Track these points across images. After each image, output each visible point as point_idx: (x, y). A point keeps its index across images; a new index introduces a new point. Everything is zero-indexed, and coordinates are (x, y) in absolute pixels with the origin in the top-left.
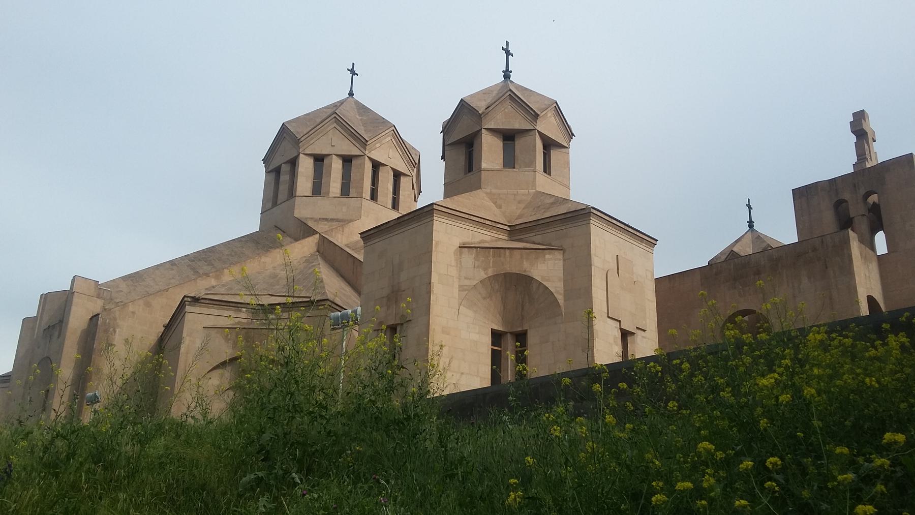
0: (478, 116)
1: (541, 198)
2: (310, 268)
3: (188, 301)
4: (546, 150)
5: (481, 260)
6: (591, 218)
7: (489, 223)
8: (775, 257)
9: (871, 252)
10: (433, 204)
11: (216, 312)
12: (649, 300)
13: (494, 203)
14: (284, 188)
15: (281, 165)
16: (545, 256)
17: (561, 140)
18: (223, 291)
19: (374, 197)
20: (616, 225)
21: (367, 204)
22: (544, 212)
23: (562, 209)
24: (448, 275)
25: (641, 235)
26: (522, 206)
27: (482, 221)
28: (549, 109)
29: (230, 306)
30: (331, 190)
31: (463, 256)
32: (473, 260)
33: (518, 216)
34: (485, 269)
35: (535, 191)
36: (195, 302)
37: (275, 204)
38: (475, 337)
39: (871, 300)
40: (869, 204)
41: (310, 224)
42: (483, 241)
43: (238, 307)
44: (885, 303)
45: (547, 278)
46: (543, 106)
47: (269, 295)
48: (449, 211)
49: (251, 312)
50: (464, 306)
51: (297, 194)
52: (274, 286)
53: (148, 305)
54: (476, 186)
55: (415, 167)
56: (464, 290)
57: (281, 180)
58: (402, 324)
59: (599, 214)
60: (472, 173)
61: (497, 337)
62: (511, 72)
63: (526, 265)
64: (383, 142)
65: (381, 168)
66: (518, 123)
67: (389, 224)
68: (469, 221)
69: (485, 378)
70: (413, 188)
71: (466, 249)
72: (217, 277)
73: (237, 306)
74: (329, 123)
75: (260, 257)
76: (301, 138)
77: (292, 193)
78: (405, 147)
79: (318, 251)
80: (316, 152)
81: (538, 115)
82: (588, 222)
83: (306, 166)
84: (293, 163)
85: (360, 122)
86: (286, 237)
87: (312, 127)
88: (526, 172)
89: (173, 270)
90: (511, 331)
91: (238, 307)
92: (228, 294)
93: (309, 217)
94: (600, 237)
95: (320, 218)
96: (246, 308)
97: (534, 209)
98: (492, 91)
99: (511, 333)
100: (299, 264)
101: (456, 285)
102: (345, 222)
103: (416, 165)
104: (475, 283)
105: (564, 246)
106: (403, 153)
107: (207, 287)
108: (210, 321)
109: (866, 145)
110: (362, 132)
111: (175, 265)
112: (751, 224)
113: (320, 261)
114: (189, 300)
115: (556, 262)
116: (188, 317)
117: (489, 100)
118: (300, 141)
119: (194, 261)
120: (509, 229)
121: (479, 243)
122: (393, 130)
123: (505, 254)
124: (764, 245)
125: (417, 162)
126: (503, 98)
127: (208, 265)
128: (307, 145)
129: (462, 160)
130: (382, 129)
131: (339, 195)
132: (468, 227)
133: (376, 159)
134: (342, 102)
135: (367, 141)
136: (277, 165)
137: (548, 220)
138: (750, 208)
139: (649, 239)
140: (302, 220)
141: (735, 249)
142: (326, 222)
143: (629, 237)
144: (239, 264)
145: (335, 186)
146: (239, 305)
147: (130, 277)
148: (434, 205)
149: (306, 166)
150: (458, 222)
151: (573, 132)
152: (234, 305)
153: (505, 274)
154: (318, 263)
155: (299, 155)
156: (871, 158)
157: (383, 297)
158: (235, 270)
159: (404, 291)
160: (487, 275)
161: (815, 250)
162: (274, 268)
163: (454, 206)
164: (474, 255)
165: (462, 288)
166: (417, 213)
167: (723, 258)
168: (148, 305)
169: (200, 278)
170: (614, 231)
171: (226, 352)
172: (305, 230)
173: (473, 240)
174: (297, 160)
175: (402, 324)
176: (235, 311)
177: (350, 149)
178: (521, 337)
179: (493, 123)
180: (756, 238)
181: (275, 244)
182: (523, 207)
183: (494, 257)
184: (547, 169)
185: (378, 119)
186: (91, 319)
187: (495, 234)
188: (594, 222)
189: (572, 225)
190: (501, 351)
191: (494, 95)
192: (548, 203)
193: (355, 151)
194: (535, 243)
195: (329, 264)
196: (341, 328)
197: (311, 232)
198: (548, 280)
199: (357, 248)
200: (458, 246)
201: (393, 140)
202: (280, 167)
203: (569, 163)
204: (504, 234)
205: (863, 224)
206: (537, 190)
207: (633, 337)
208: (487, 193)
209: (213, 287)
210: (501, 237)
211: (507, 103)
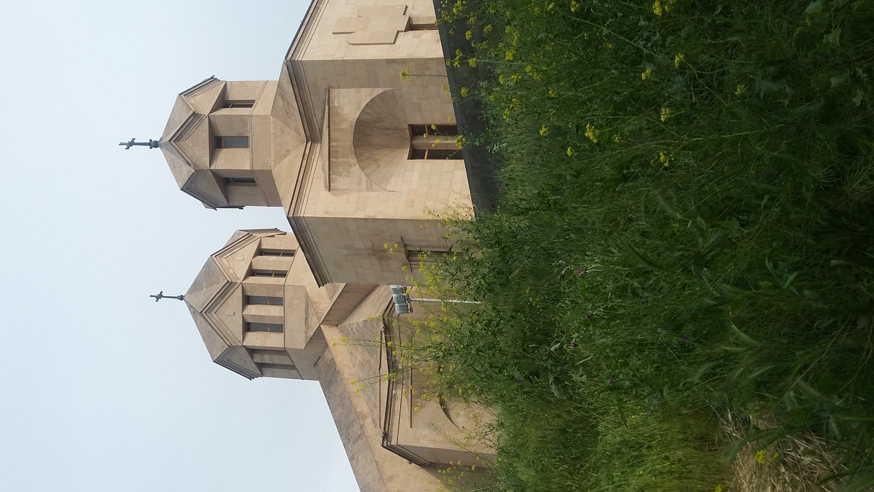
1: (277, 109)
2: (354, 333)
3: (387, 443)
5: (342, 170)
6: (296, 59)
7: (305, 162)
10: (288, 218)
11: (396, 417)
13: (285, 158)
14: (277, 360)
15: (255, 362)
16: (336, 107)
17: (217, 91)
19: (283, 274)
20: (302, 35)
21: (290, 280)
22: (292, 107)
23: (289, 89)
25: (312, 9)
26: (286, 128)
27: (303, 169)
28: (187, 101)
31: (338, 188)
32: (342, 177)
33: (296, 133)
34: (351, 166)
35: (271, 117)
36: (388, 436)
37: (293, 367)
42: (323, 169)
43: (392, 397)
47: (380, 369)
48: (294, 201)
51: (283, 346)
52: (371, 365)
53: (391, 479)
54: (268, 175)
55: (252, 235)
56: (371, 185)
57: (269, 362)
58: (405, 245)
59: (292, 52)
60: (256, 181)
61: (416, 154)
62: (151, 140)
63: (345, 126)
64: (227, 265)
65: (254, 268)
66: (203, 133)
67: (309, 259)
68: (303, 182)
69: (455, 166)
70: (273, 236)
71: (331, 184)
72: (364, 417)
73: (390, 398)
74: (211, 319)
75: (344, 379)
77: (282, 352)
80: (241, 330)
81: (194, 113)
82: (300, 63)
83: (255, 339)
84: (252, 351)
85: (208, 289)
86: (324, 356)
87: (216, 334)
89: (358, 457)
90: (410, 141)
91: (392, 397)
92: (380, 407)
93: (304, 335)
95: (306, 324)
96: (392, 390)
97: (289, 117)
98: (171, 160)
99: (412, 140)
101: (366, 194)
102: (308, 301)
103: (250, 234)
104: (364, 177)
105: (326, 88)
106: (238, 247)
107: (374, 426)
108: (406, 422)
113: (347, 323)
114: (385, 442)
115: (341, 95)
116: (402, 442)
117: (181, 162)
120: (310, 142)
121: (325, 171)
126: (177, 148)
127: (352, 426)
128: (234, 338)
129: (244, 189)
131: (282, 307)
132: (310, 183)
134: (190, 307)
135: (228, 281)
142: (309, 319)
143: (314, 21)
144: (351, 398)
145: (272, 312)
146: (390, 396)
148: (289, 216)
149: (255, 339)
150: (304, 192)
151: (210, 77)
152: (390, 402)
154: (349, 326)
155: (245, 347)
157: (380, 263)
158: (356, 401)
159: (373, 244)
160: (356, 164)
163: (289, 196)
164: (337, 177)
165: (369, 188)
166: (297, 233)
168: (391, 479)
169: (366, 433)
171: (434, 406)
174: (249, 348)
175: (405, 245)
176: (395, 400)
177: (237, 296)
178: (416, 131)
179: (204, 159)
181: (332, 366)
182: (287, 128)
184: (249, 104)
185: (206, 272)
187: (316, 157)
188: (299, 57)
189: (305, 80)
190: (429, 150)
192: (283, 103)
193: (238, 293)
194: (323, 118)
195: (349, 315)
197: (319, 333)
198: (360, 105)
201: (225, 256)
204: (316, 147)
206: (269, 114)
207: (413, 19)
208: (275, 165)
209: (374, 420)
210: (318, 151)
211: (183, 144)
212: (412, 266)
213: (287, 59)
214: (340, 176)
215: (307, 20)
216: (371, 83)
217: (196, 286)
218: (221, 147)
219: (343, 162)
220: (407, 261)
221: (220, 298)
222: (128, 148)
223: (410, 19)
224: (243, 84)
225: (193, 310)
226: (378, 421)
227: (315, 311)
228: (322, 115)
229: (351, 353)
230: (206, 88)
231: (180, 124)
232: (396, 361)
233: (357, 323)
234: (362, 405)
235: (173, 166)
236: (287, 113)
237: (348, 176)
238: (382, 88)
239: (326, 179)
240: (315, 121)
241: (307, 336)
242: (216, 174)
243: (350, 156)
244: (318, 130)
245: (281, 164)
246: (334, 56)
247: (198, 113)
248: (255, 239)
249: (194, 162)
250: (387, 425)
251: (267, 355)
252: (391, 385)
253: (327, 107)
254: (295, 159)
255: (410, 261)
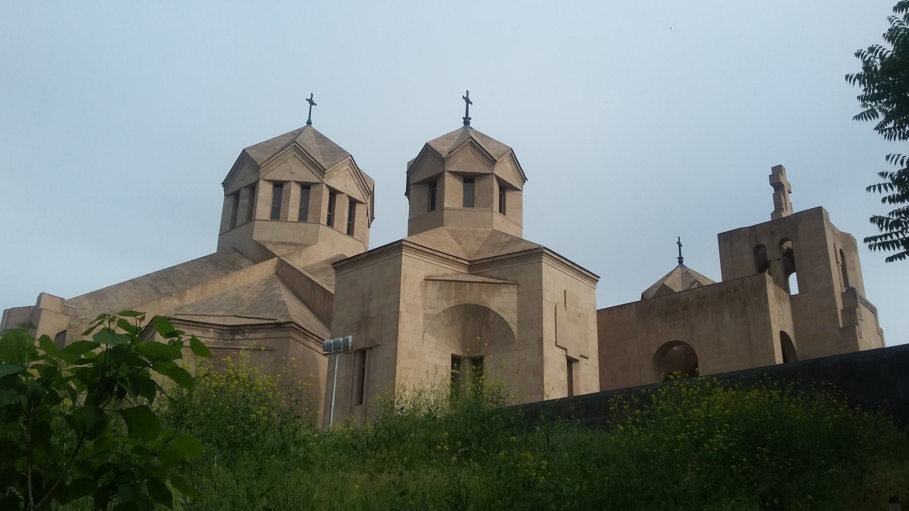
0: (441, 160)
1: (499, 236)
2: (270, 291)
4: (501, 192)
5: (444, 292)
6: (543, 257)
8: (701, 295)
9: (785, 293)
10: (402, 240)
12: (591, 330)
14: (242, 212)
15: (241, 189)
18: (190, 311)
19: (330, 223)
21: (324, 229)
22: (501, 249)
23: (517, 248)
24: (414, 305)
25: (586, 273)
26: (481, 243)
27: (445, 256)
28: (506, 155)
29: (199, 326)
30: (290, 215)
31: (428, 288)
32: (437, 292)
33: (477, 252)
34: (448, 300)
35: (491, 229)
37: (233, 226)
38: (436, 361)
39: (783, 335)
40: (784, 249)
41: (269, 247)
42: (445, 275)
44: (796, 338)
45: (503, 309)
46: (501, 153)
47: (235, 316)
49: (218, 333)
50: (428, 333)
51: (256, 218)
54: (439, 223)
55: (369, 195)
58: (371, 348)
59: (550, 253)
60: (434, 211)
61: (455, 360)
62: (470, 119)
63: (484, 297)
64: (341, 170)
65: (338, 196)
66: (478, 167)
67: (360, 256)
70: (367, 216)
72: (180, 297)
75: (221, 278)
76: (262, 164)
77: (251, 216)
78: (359, 174)
79: (276, 274)
80: (276, 179)
81: (496, 161)
83: (265, 191)
84: (253, 188)
88: (485, 212)
89: (135, 289)
92: (196, 315)
93: (267, 240)
94: (551, 274)
95: (278, 242)
98: (453, 136)
99: (469, 358)
100: (259, 286)
101: (422, 314)
103: (371, 194)
104: (437, 312)
107: (175, 308)
109: (782, 196)
110: (321, 161)
111: (137, 283)
112: (681, 260)
115: (511, 295)
117: (451, 145)
118: (260, 167)
119: (155, 280)
120: (469, 264)
122: (350, 160)
123: (466, 287)
124: (692, 280)
125: (372, 190)
126: (465, 144)
127: (170, 284)
128: (268, 171)
130: (340, 158)
131: (296, 220)
133: (333, 187)
134: (300, 131)
135: (325, 170)
136: (236, 189)
137: (504, 257)
138: (680, 245)
139: (593, 276)
140: (262, 244)
141: (666, 283)
142: (284, 246)
144: (201, 285)
145: (293, 211)
146: (207, 326)
147: (93, 295)
149: (265, 191)
150: (424, 256)
151: (526, 176)
152: (202, 325)
153: (465, 305)
154: (278, 286)
155: (258, 181)
156: (786, 208)
157: (353, 323)
158: (198, 289)
161: (736, 290)
162: (236, 289)
164: (437, 288)
165: (426, 317)
167: (656, 290)
170: (562, 268)
172: (264, 253)
173: (437, 274)
174: (257, 185)
175: (371, 348)
178: (477, 362)
179: (455, 166)
180: (685, 273)
183: (455, 289)
184: (502, 210)
186: (57, 335)
187: (456, 268)
188: (545, 259)
191: (455, 140)
193: (313, 179)
196: (333, 354)
197: (269, 255)
198: (503, 312)
199: (313, 272)
200: (424, 278)
201: (350, 169)
202: (239, 191)
203: (521, 204)
205: (777, 267)
206: (494, 228)
207: (577, 364)
208: (448, 230)
209: (182, 308)
210: (461, 271)
212: (350, 354)
213: (544, 249)
214: (438, 290)
215: (577, 268)
216: (521, 323)
217: (320, 138)
218: (464, 182)
219: (452, 294)
220: (355, 349)
221: (309, 160)
222: (464, 98)
223: (577, 361)
224: (520, 205)
225: (297, 133)
226: (181, 313)
227: (293, 252)
228: (494, 277)
229: (249, 287)
230: (516, 172)
231: (483, 144)
232: (244, 333)
233: (280, 295)
234: (192, 297)
235: (448, 137)
236: (496, 245)
237: (438, 298)
238: (518, 333)
239: (436, 277)
240: (490, 269)
241: (267, 243)
242: (441, 175)
243: (456, 300)
244: (480, 271)
245: (448, 235)
246: (546, 291)
247: (495, 164)
248: (367, 200)
249: (452, 157)
250: (177, 322)
251: (247, 203)
252: (219, 327)
253: (501, 281)
254: (453, 248)
255: (355, 352)
